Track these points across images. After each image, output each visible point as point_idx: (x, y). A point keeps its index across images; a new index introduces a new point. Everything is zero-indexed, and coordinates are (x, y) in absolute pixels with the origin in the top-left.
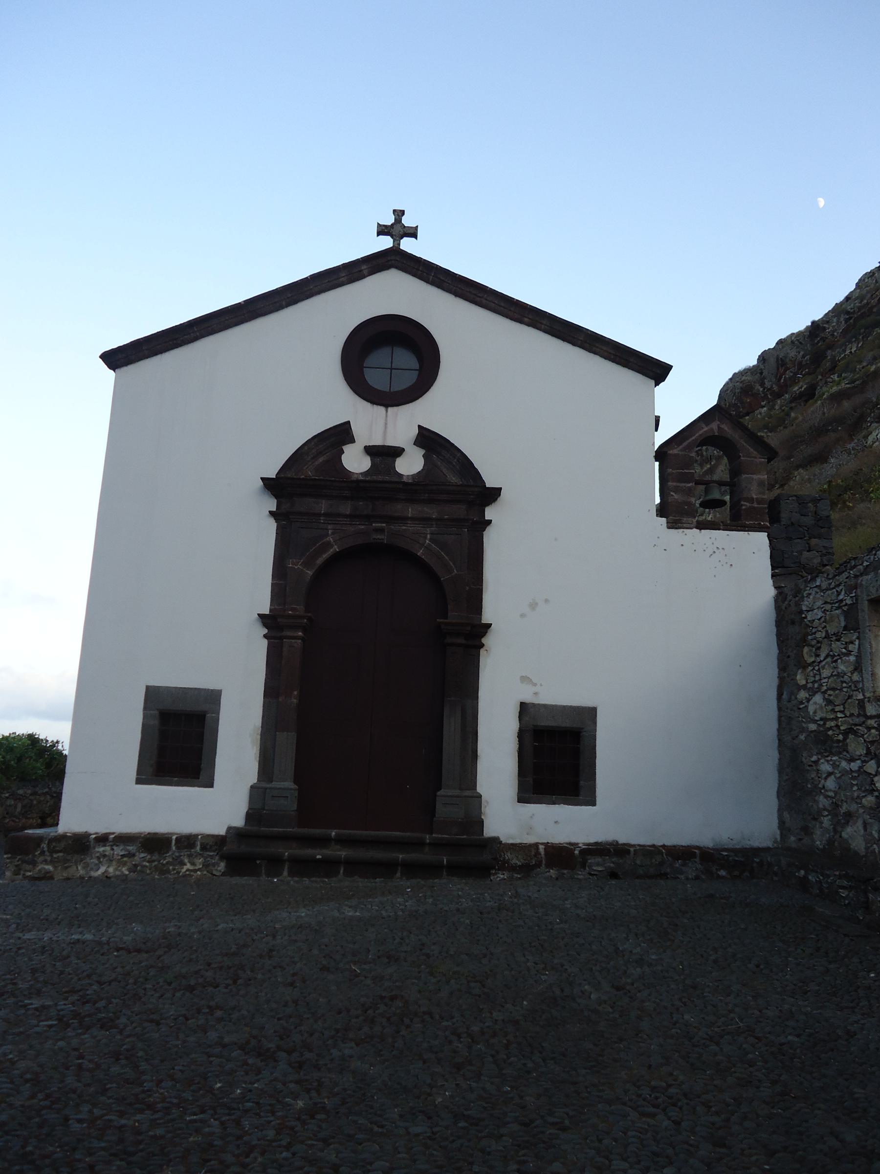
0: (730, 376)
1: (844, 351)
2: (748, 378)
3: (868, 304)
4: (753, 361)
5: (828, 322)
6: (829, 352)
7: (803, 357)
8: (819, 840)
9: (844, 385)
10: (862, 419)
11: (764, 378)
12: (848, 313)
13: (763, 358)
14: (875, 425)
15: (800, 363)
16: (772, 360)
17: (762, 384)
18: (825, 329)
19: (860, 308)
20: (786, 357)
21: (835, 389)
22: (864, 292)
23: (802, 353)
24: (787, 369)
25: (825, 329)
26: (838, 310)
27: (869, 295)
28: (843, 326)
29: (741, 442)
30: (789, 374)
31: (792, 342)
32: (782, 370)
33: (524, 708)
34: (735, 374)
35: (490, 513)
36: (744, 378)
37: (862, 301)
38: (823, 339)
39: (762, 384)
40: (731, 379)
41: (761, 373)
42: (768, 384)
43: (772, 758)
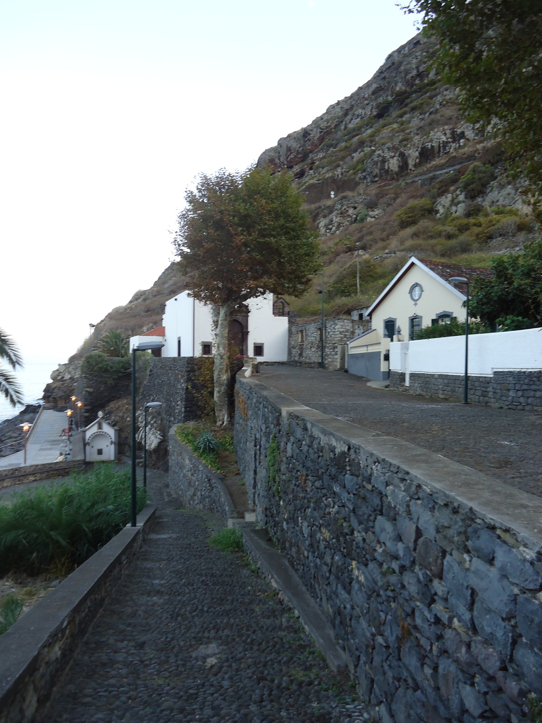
0: (264, 151)
1: (317, 156)
2: (272, 154)
3: (330, 126)
4: (275, 144)
5: (312, 130)
6: (310, 155)
7: (299, 148)
8: (292, 360)
9: (314, 181)
10: (317, 214)
11: (280, 156)
12: (321, 128)
13: (281, 142)
14: (322, 219)
15: (298, 151)
16: (285, 147)
17: (279, 159)
18: (310, 134)
19: (327, 127)
20: (291, 146)
21: (311, 182)
22: (329, 117)
23: (299, 145)
24: (291, 153)
25: (310, 134)
26: (316, 122)
27: (331, 122)
28: (318, 135)
29: (285, 303)
30: (292, 156)
31: (295, 138)
32: (289, 153)
33: (255, 343)
34: (266, 150)
35: (249, 314)
36: (270, 154)
37: (328, 123)
38: (309, 140)
39: (279, 159)
40: (264, 152)
41: (279, 153)
42: (282, 159)
43: (287, 350)
